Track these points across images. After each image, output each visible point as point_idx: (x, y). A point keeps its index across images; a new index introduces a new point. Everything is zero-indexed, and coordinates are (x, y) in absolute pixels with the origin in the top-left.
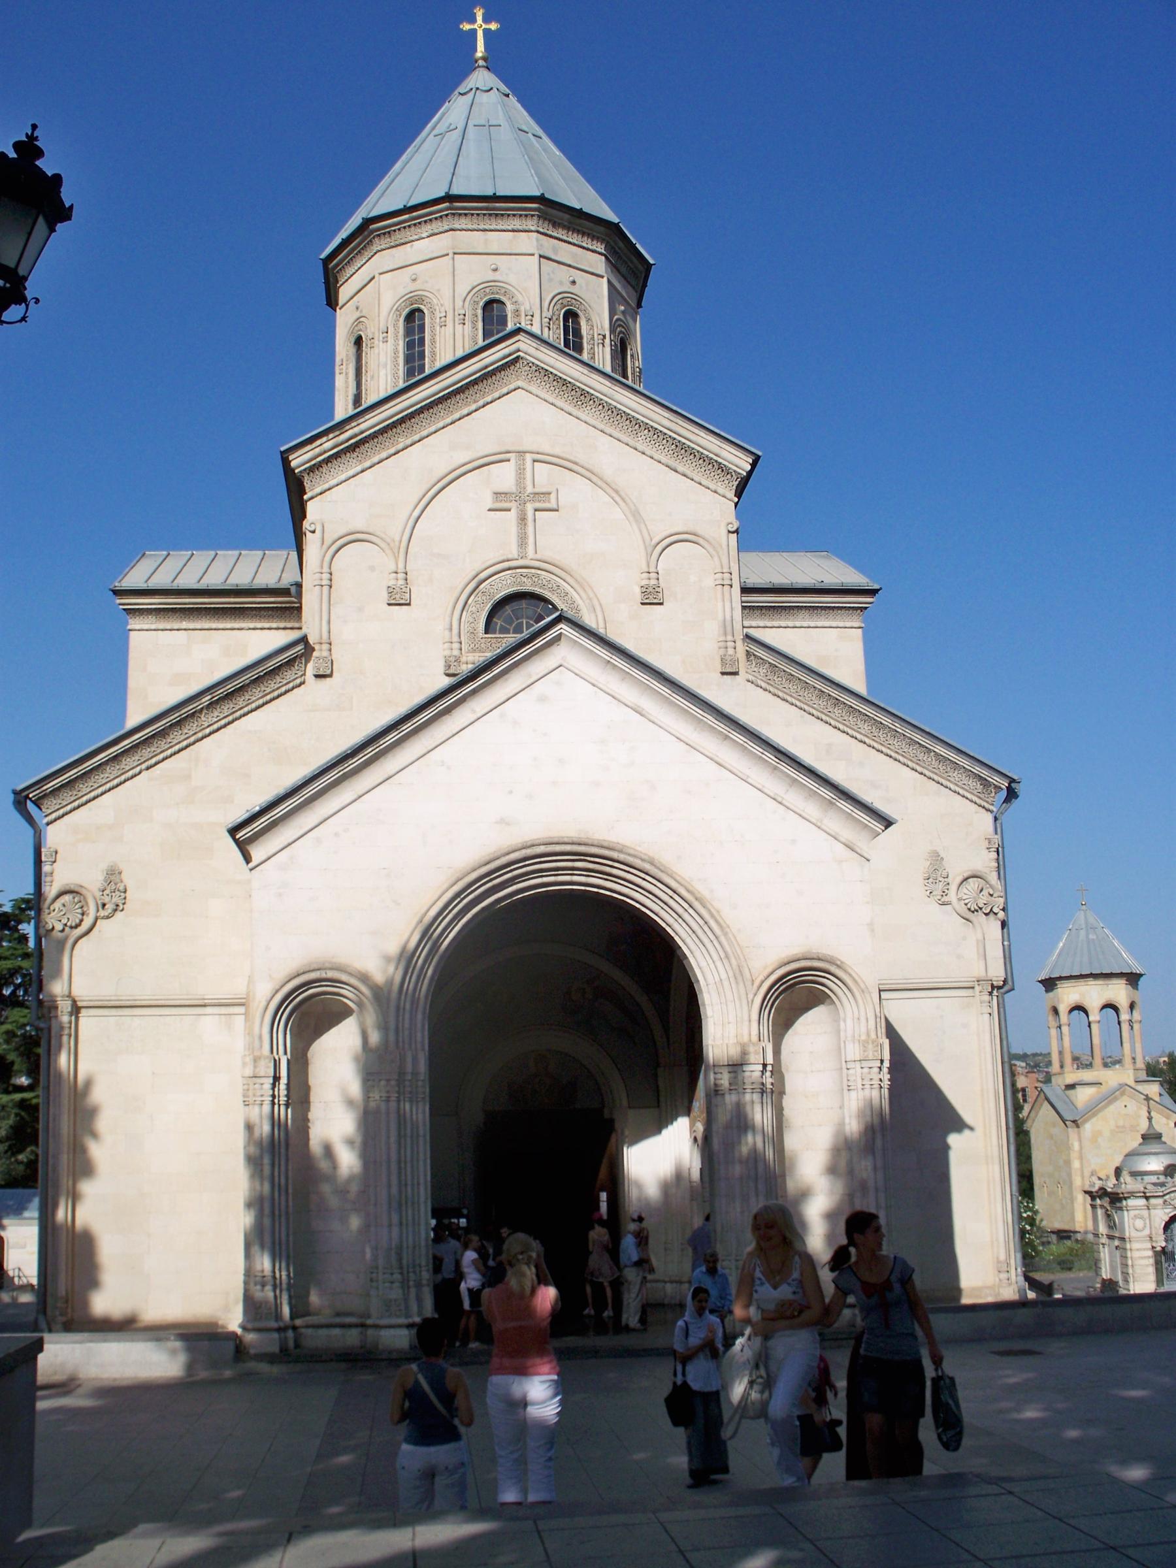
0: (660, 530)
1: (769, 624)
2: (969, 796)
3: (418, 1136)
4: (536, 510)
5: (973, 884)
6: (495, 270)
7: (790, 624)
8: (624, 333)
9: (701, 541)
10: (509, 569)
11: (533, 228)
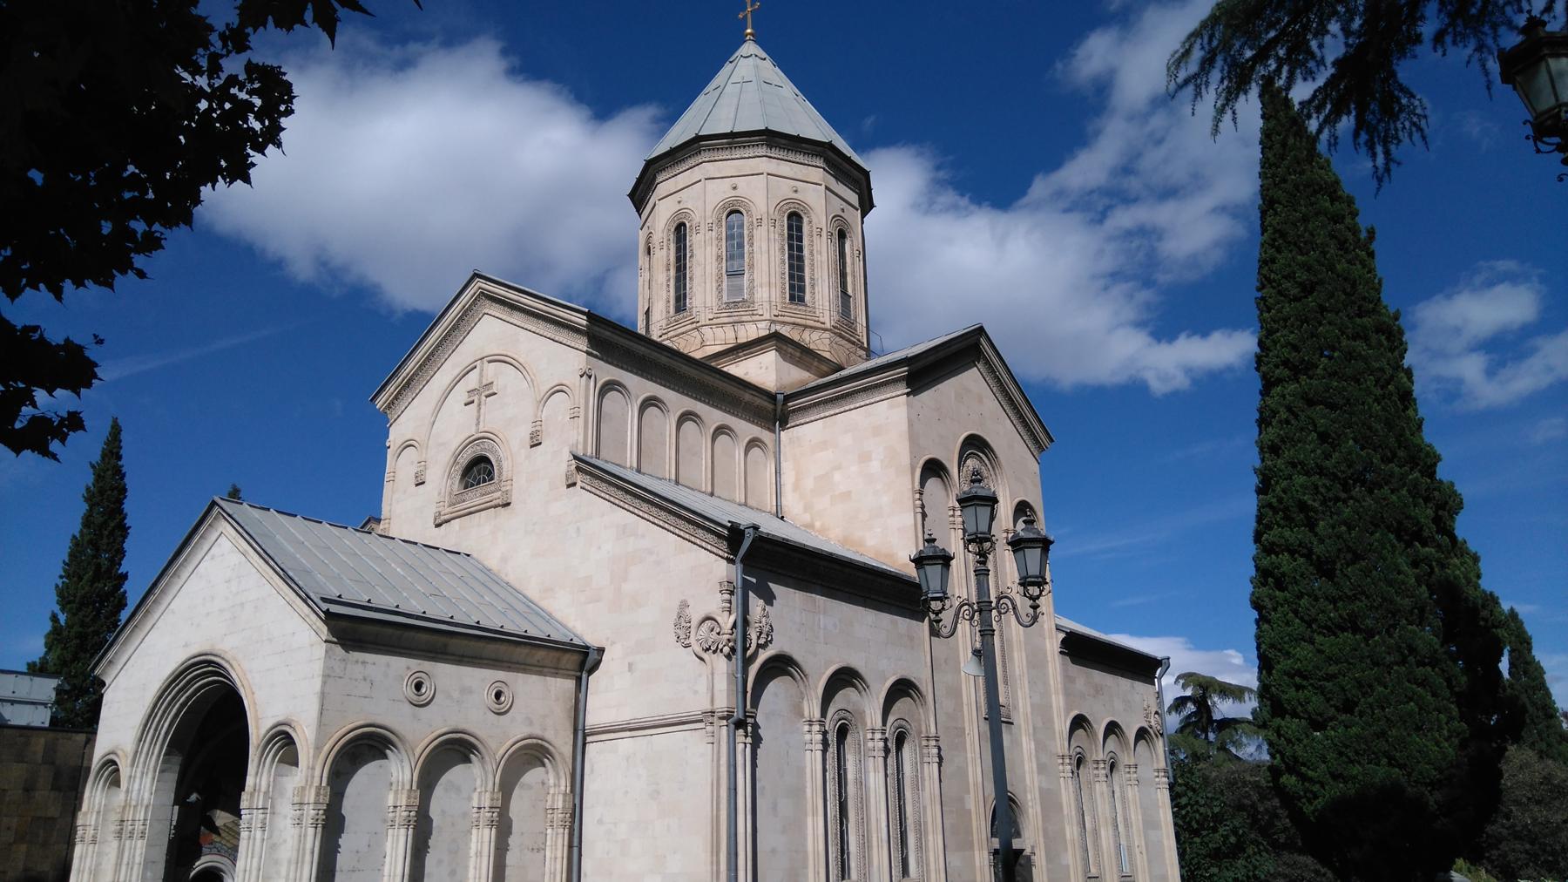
0: (545, 388)
1: (837, 411)
2: (709, 547)
3: (133, 863)
4: (487, 397)
5: (708, 623)
6: (679, 202)
7: (852, 407)
8: (795, 208)
9: (564, 388)
10: (471, 443)
11: (700, 161)
